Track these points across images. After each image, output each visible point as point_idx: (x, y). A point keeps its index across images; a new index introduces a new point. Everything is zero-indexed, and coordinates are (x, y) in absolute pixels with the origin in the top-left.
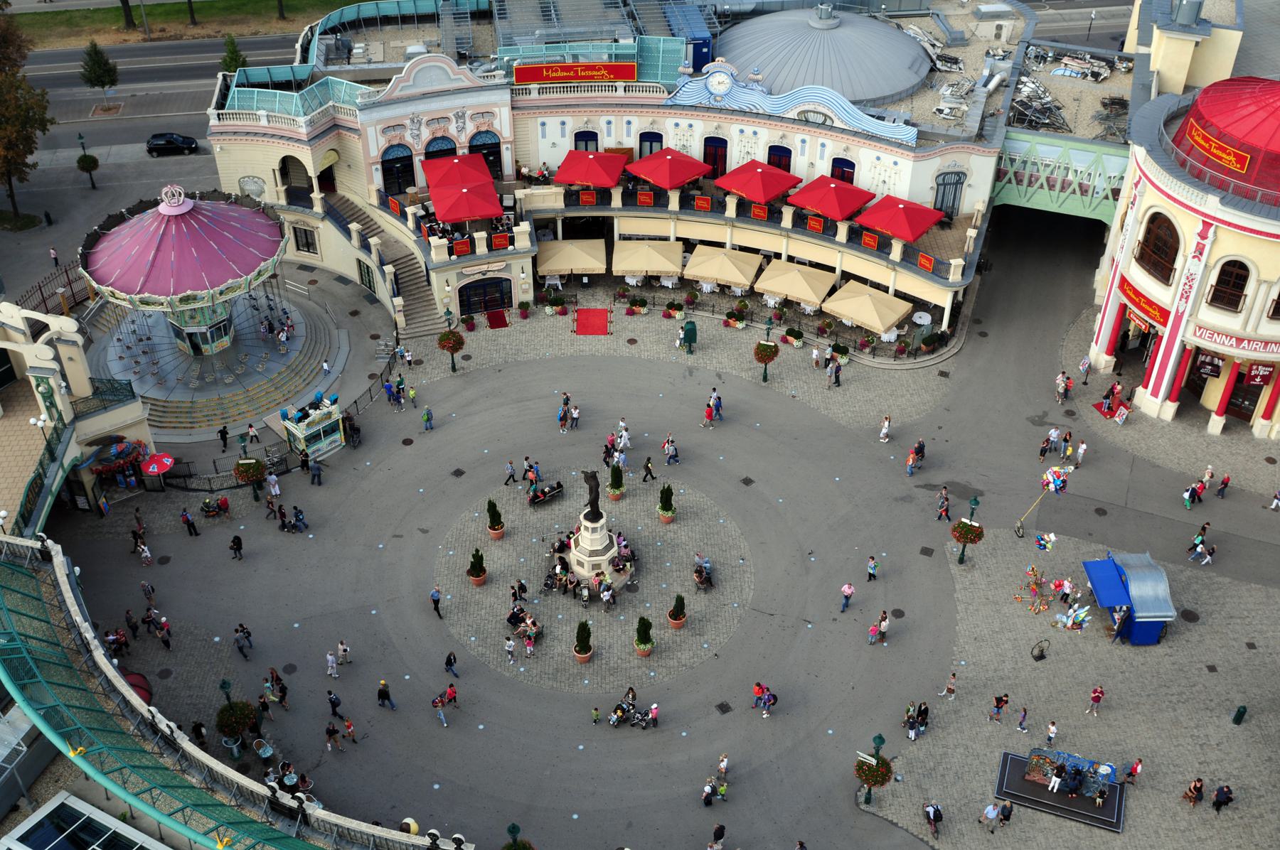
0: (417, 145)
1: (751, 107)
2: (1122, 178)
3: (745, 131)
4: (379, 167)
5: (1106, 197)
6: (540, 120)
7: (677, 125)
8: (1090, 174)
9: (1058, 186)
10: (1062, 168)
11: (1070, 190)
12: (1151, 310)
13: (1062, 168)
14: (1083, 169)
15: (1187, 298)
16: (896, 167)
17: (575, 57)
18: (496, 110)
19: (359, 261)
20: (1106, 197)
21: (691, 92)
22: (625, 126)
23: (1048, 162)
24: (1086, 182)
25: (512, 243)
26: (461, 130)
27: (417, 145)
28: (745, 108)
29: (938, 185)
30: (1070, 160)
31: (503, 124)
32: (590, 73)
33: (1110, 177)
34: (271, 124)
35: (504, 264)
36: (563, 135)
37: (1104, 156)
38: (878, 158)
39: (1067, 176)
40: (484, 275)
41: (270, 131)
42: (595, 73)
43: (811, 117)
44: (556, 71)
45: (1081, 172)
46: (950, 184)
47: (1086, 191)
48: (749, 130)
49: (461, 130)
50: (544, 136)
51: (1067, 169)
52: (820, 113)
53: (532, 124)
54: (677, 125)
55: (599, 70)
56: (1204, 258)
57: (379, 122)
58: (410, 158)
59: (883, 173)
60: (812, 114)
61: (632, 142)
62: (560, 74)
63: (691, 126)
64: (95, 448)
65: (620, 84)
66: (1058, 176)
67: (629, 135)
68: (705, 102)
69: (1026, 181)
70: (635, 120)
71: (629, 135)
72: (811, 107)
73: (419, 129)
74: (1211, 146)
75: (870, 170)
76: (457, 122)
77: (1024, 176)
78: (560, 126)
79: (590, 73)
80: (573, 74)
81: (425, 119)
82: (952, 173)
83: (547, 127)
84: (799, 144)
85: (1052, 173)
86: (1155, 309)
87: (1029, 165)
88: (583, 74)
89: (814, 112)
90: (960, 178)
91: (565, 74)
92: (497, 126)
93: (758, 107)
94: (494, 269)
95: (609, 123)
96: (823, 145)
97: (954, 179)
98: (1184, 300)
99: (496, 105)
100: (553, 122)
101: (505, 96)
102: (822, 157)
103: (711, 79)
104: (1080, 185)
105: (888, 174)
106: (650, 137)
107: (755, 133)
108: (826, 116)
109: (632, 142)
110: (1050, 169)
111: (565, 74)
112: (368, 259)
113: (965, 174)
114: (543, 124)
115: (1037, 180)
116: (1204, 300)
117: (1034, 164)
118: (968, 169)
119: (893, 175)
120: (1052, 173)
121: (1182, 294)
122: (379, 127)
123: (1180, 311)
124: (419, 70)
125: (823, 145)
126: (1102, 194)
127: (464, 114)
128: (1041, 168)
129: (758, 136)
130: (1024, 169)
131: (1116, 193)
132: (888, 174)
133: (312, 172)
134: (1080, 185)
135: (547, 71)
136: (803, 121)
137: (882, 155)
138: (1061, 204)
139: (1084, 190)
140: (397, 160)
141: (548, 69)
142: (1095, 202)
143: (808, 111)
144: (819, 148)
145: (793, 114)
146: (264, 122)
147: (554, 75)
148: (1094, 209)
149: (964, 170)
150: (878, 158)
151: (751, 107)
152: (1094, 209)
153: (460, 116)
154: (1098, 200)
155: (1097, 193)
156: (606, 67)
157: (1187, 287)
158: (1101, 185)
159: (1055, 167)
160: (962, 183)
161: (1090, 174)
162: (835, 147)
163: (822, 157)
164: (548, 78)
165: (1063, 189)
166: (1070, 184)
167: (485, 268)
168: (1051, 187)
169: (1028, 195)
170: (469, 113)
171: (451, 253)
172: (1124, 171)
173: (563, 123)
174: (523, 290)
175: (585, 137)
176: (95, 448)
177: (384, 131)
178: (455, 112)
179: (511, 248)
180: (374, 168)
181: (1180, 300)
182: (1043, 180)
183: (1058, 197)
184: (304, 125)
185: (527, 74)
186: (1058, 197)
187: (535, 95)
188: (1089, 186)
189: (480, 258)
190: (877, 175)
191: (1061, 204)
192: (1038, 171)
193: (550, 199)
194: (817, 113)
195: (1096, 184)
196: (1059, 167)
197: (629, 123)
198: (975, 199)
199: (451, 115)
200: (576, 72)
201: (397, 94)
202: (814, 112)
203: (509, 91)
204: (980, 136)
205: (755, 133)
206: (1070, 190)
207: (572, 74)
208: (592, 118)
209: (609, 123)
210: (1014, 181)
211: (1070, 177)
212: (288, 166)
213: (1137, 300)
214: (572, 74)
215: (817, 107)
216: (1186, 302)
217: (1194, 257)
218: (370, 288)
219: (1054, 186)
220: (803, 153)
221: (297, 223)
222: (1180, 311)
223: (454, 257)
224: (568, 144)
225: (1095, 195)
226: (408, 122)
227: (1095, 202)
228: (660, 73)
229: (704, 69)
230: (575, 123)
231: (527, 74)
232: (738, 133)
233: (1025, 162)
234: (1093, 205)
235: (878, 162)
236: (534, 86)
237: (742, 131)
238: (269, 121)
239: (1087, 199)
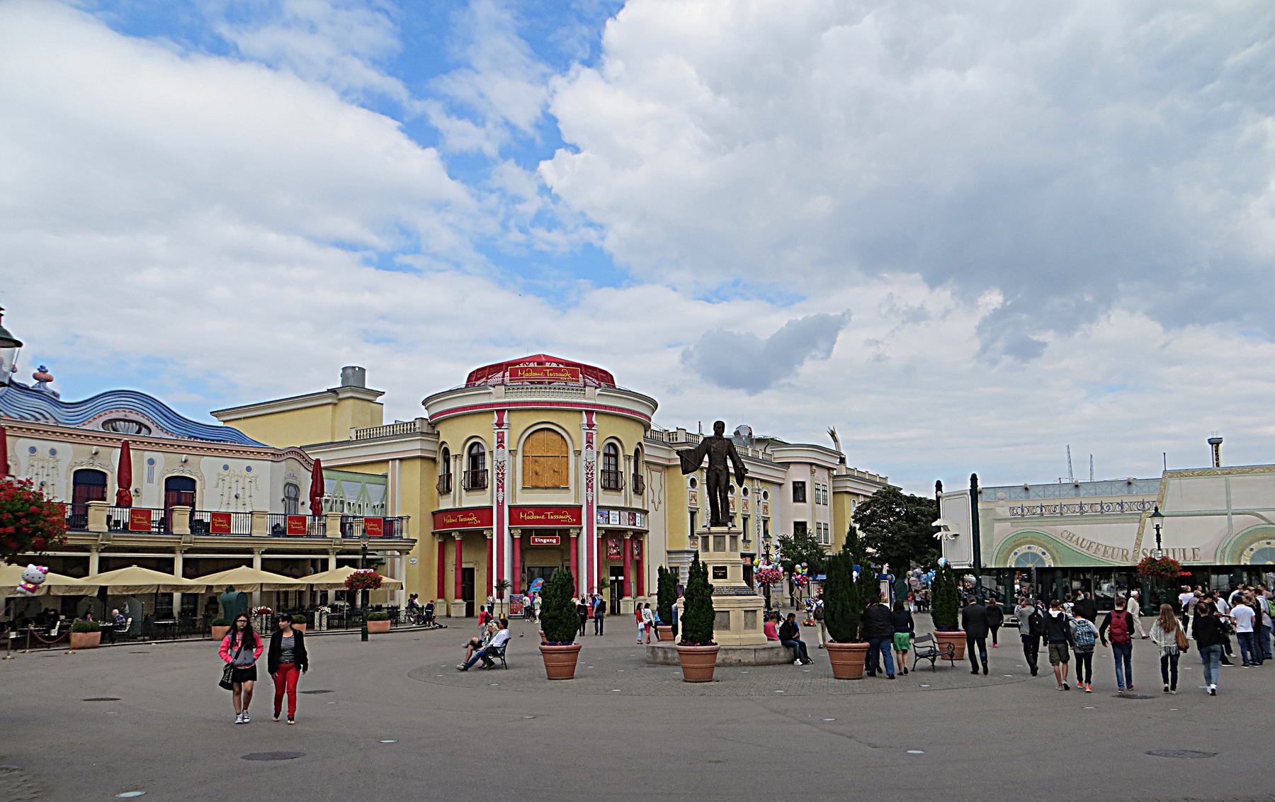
1: (38, 416)
3: (39, 449)
8: (360, 506)
10: (339, 502)
12: (561, 517)
13: (339, 502)
15: (592, 488)
28: (28, 416)
30: (343, 492)
33: (374, 507)
37: (367, 485)
38: (226, 468)
48: (43, 447)
51: (342, 502)
52: (132, 421)
56: (594, 445)
59: (234, 485)
60: (122, 423)
72: (121, 415)
86: (565, 514)
89: (125, 421)
93: (48, 416)
96: (151, 462)
98: (589, 489)
102: (150, 480)
105: (240, 485)
107: (53, 452)
110: (330, 502)
119: (247, 486)
121: (587, 484)
125: (151, 462)
129: (58, 456)
132: (240, 485)
144: (146, 465)
151: (38, 416)
157: (589, 476)
161: (360, 506)
163: (150, 480)
181: (587, 491)
190: (226, 489)
202: (125, 421)
213: (543, 517)
215: (127, 414)
216: (592, 491)
222: (590, 501)
232: (28, 453)
235: (226, 473)
237: (33, 450)
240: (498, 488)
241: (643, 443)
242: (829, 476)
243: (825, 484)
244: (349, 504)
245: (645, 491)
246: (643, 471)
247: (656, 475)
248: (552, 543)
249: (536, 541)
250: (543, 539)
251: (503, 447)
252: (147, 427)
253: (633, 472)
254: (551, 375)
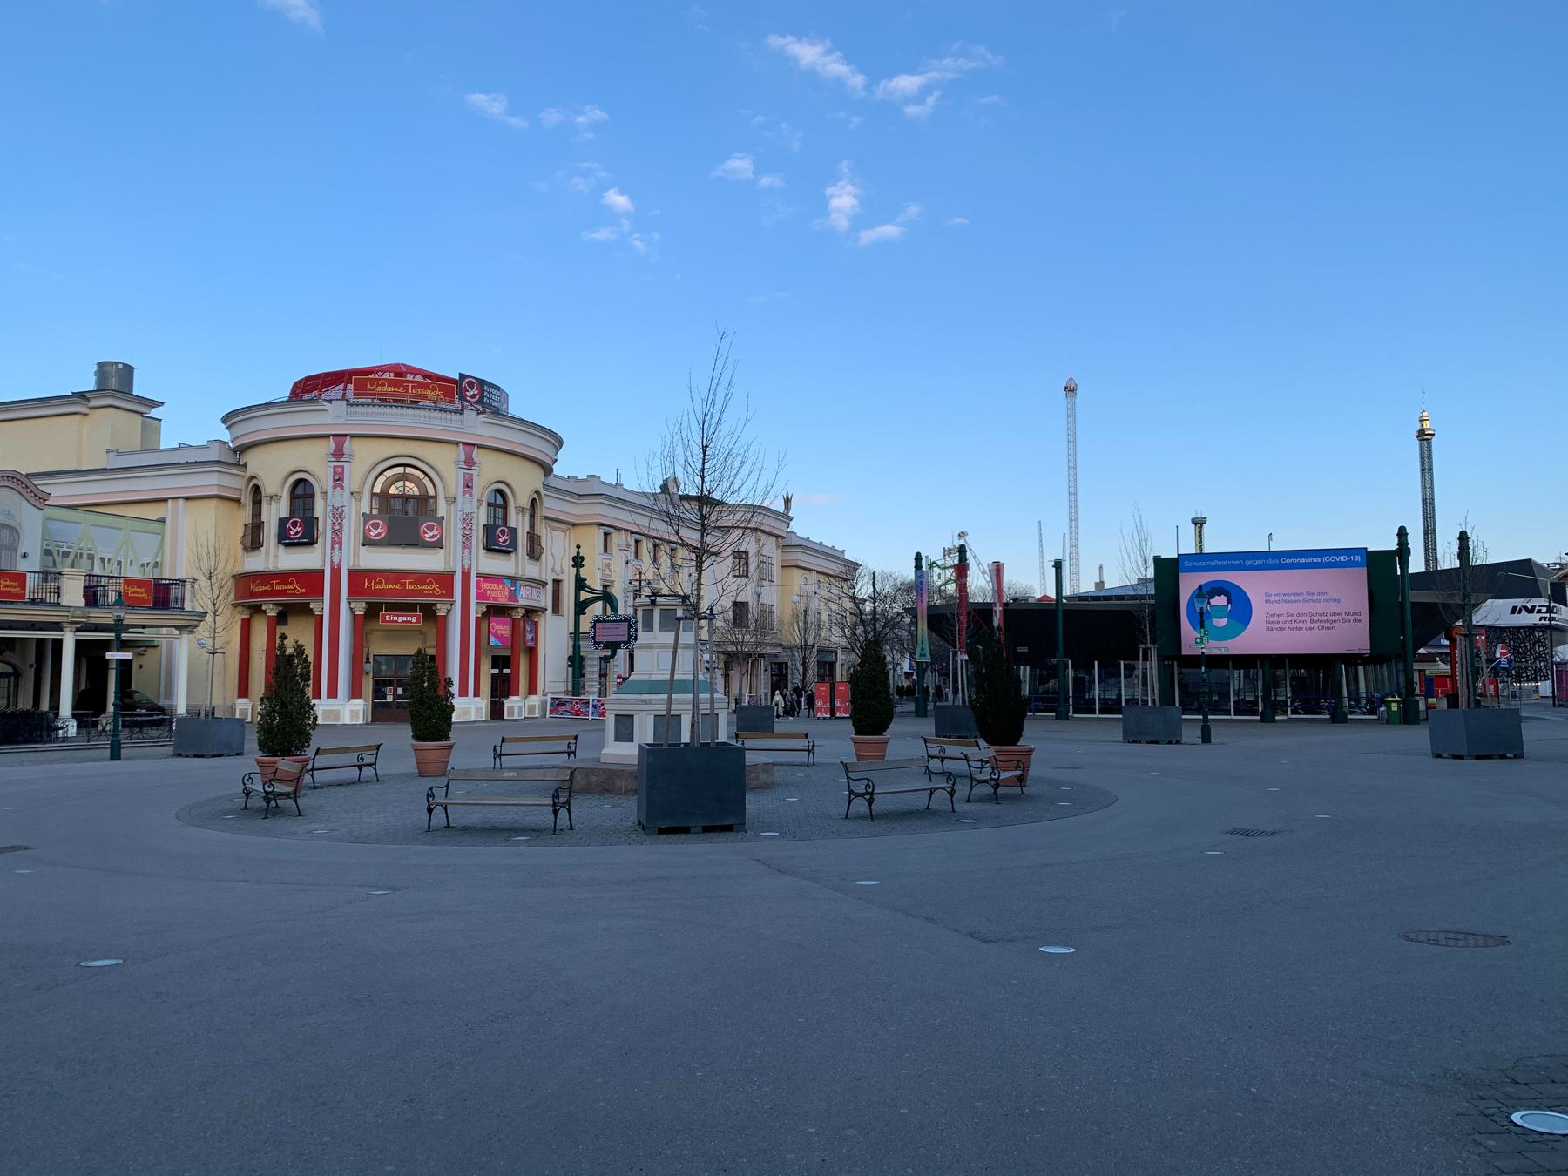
8: (119, 563)
10: (85, 556)
12: (425, 587)
13: (85, 556)
14: (110, 556)
23: (65, 549)
33: (143, 565)
39: (92, 569)
45: (109, 560)
51: (91, 557)
74: (406, 388)
98: (466, 551)
110: (72, 556)
116: (481, 546)
123: (466, 567)
159: (76, 555)
161: (119, 563)
181: (463, 553)
196: (81, 554)
213: (398, 586)
216: (470, 553)
217: (464, 493)
222: (466, 567)
240: (333, 544)
241: (543, 492)
242: (778, 547)
243: (771, 555)
244: (102, 559)
245: (543, 556)
246: (542, 529)
247: (559, 536)
248: (410, 622)
249: (387, 619)
250: (398, 616)
251: (342, 488)
253: (527, 529)
254: (415, 391)
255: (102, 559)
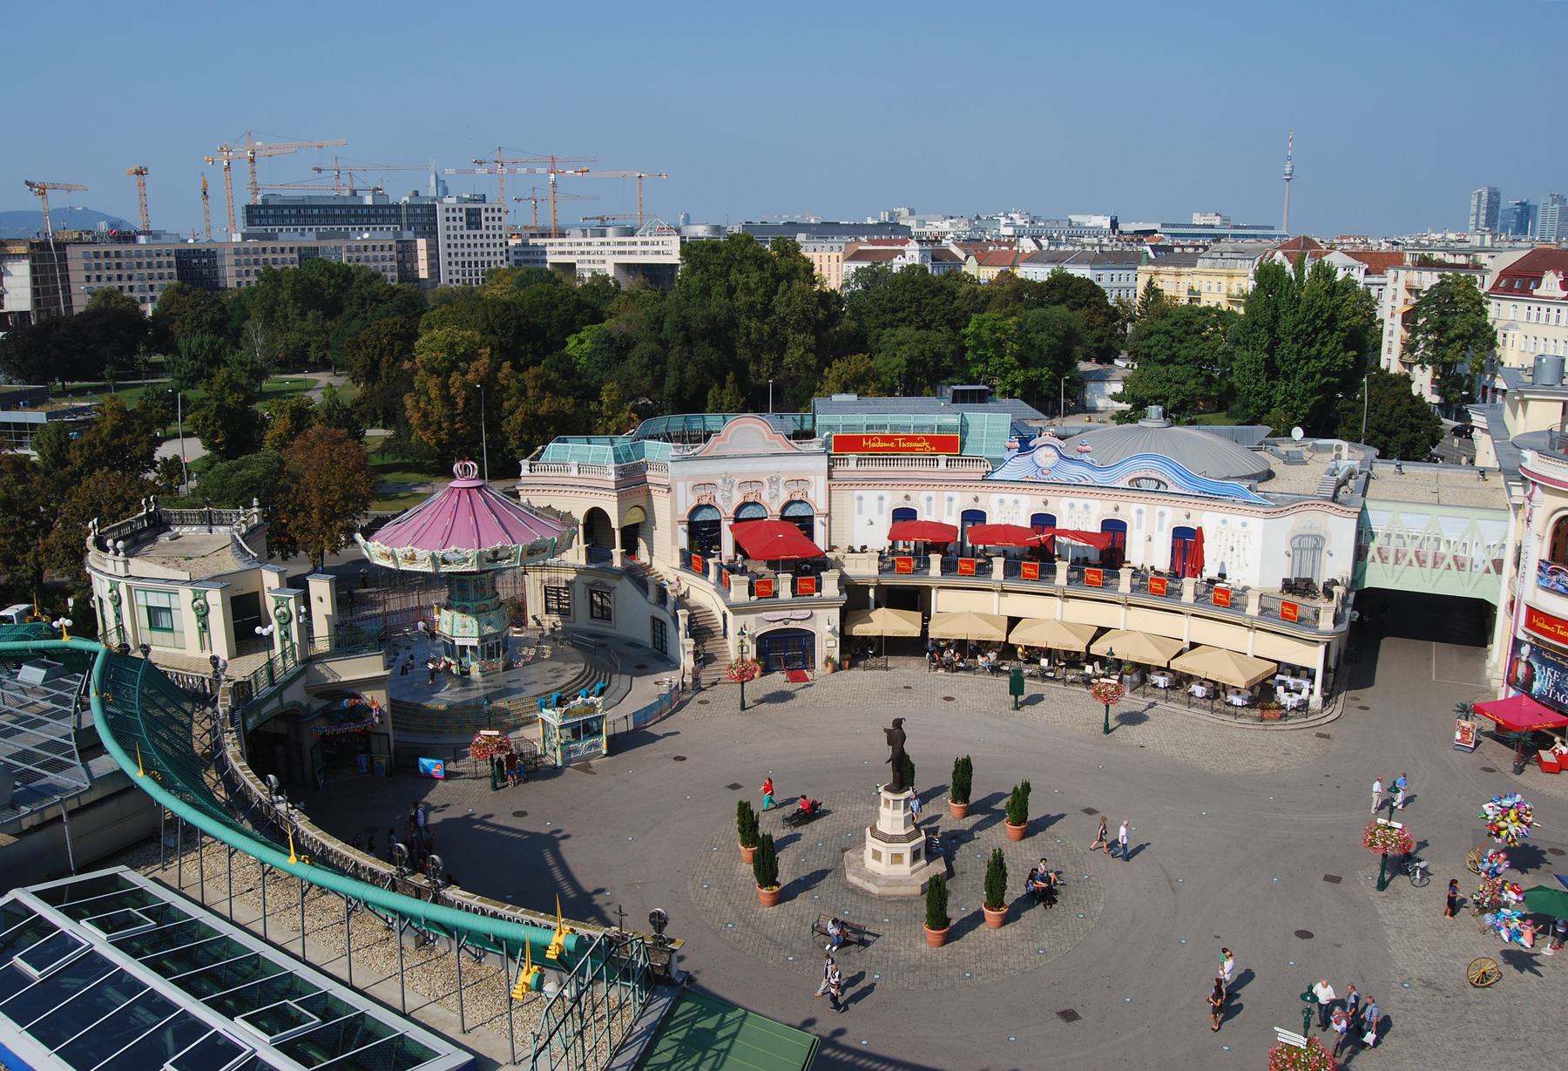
0: (726, 509)
2: (1503, 546)
4: (685, 527)
5: (1488, 571)
6: (857, 493)
7: (1002, 501)
8: (1465, 544)
9: (1430, 562)
10: (1432, 539)
11: (1444, 565)
13: (1432, 539)
16: (1245, 530)
17: (895, 427)
18: (811, 478)
19: (654, 619)
20: (1488, 571)
21: (1016, 467)
22: (946, 503)
24: (1461, 554)
25: (819, 590)
26: (774, 497)
27: (726, 509)
29: (1293, 549)
31: (817, 496)
32: (911, 445)
33: (1489, 547)
34: (581, 475)
35: (808, 613)
36: (880, 512)
37: (1479, 522)
38: (1224, 522)
39: (1439, 548)
40: (786, 624)
41: (579, 482)
42: (916, 445)
43: (1144, 484)
44: (877, 441)
46: (1307, 549)
47: (1463, 565)
49: (774, 497)
50: (860, 512)
51: (1438, 540)
53: (846, 499)
54: (1002, 501)
55: (921, 441)
57: (689, 478)
58: (716, 524)
59: (1230, 538)
61: (954, 520)
62: (880, 445)
63: (1016, 502)
64: (323, 703)
65: (942, 458)
66: (1428, 550)
67: (950, 512)
68: (1032, 476)
69: (1391, 559)
70: (957, 496)
71: (950, 512)
72: (1143, 474)
73: (730, 491)
75: (1215, 538)
76: (770, 488)
77: (1388, 552)
78: (877, 502)
79: (911, 445)
80: (892, 447)
81: (737, 481)
82: (1308, 536)
83: (864, 502)
84: (1134, 516)
85: (1421, 546)
87: (1393, 538)
88: (904, 445)
89: (1146, 479)
90: (1318, 543)
91: (885, 445)
92: (811, 496)
94: (795, 618)
95: (930, 499)
97: (1309, 543)
99: (811, 472)
100: (870, 496)
101: (823, 462)
102: (1160, 529)
103: (1037, 452)
104: (1455, 558)
105: (1236, 538)
106: (973, 517)
107: (1086, 507)
108: (1159, 482)
109: (954, 520)
111: (885, 445)
112: (662, 611)
113: (1323, 539)
114: (860, 498)
115: (1404, 555)
117: (1399, 536)
118: (1326, 533)
120: (1421, 546)
122: (690, 484)
124: (736, 431)
125: (1162, 514)
126: (1482, 568)
127: (778, 480)
128: (1408, 541)
130: (1388, 544)
131: (1498, 565)
132: (1236, 538)
133: (615, 524)
134: (1455, 558)
135: (867, 441)
136: (1136, 486)
137: (1229, 517)
138: (1436, 583)
139: (1460, 566)
140: (704, 523)
141: (867, 438)
142: (1475, 577)
143: (1139, 478)
145: (1124, 483)
146: (574, 472)
147: (874, 445)
148: (1475, 586)
149: (1322, 534)
150: (1224, 522)
152: (1475, 586)
153: (773, 481)
154: (1480, 574)
155: (1476, 566)
156: (928, 439)
158: (1481, 557)
160: (1321, 549)
162: (1176, 515)
163: (1160, 529)
164: (867, 449)
165: (1435, 564)
166: (1443, 558)
167: (787, 614)
168: (1422, 563)
169: (1396, 574)
170: (784, 479)
171: (751, 594)
172: (1505, 537)
173: (881, 498)
174: (827, 645)
175: (903, 516)
176: (323, 703)
177: (694, 488)
178: (769, 477)
179: (817, 595)
180: (680, 527)
182: (1411, 555)
183: (1431, 575)
184: (613, 472)
185: (846, 444)
186: (1431, 575)
187: (853, 465)
188: (1465, 559)
189: (783, 602)
191: (1436, 583)
192: (1405, 545)
193: (864, 569)
194: (1150, 479)
195: (1473, 555)
197: (951, 499)
198: (1336, 565)
199: (764, 479)
200: (897, 443)
201: (713, 453)
202: (1146, 479)
203: (825, 458)
204: (1334, 499)
205: (1086, 507)
206: (1444, 565)
207: (892, 445)
208: (911, 494)
209: (930, 499)
210: (1378, 559)
211: (1443, 549)
212: (596, 518)
213: (1552, 629)
214: (892, 445)
218: (661, 650)
219: (1424, 561)
220: (1139, 527)
221: (594, 585)
223: (754, 598)
224: (885, 523)
225: (1474, 569)
226: (719, 482)
227: (1475, 577)
228: (984, 447)
229: (1031, 444)
230: (894, 499)
231: (846, 444)
233: (1388, 536)
234: (1472, 584)
235: (1224, 527)
236: (853, 456)
237: (1072, 505)
238: (579, 472)
239: (1465, 574)
244: (1448, 542)
252: (1164, 483)
255: (1448, 542)
